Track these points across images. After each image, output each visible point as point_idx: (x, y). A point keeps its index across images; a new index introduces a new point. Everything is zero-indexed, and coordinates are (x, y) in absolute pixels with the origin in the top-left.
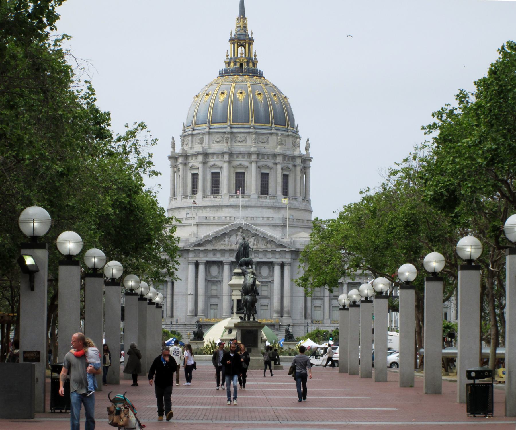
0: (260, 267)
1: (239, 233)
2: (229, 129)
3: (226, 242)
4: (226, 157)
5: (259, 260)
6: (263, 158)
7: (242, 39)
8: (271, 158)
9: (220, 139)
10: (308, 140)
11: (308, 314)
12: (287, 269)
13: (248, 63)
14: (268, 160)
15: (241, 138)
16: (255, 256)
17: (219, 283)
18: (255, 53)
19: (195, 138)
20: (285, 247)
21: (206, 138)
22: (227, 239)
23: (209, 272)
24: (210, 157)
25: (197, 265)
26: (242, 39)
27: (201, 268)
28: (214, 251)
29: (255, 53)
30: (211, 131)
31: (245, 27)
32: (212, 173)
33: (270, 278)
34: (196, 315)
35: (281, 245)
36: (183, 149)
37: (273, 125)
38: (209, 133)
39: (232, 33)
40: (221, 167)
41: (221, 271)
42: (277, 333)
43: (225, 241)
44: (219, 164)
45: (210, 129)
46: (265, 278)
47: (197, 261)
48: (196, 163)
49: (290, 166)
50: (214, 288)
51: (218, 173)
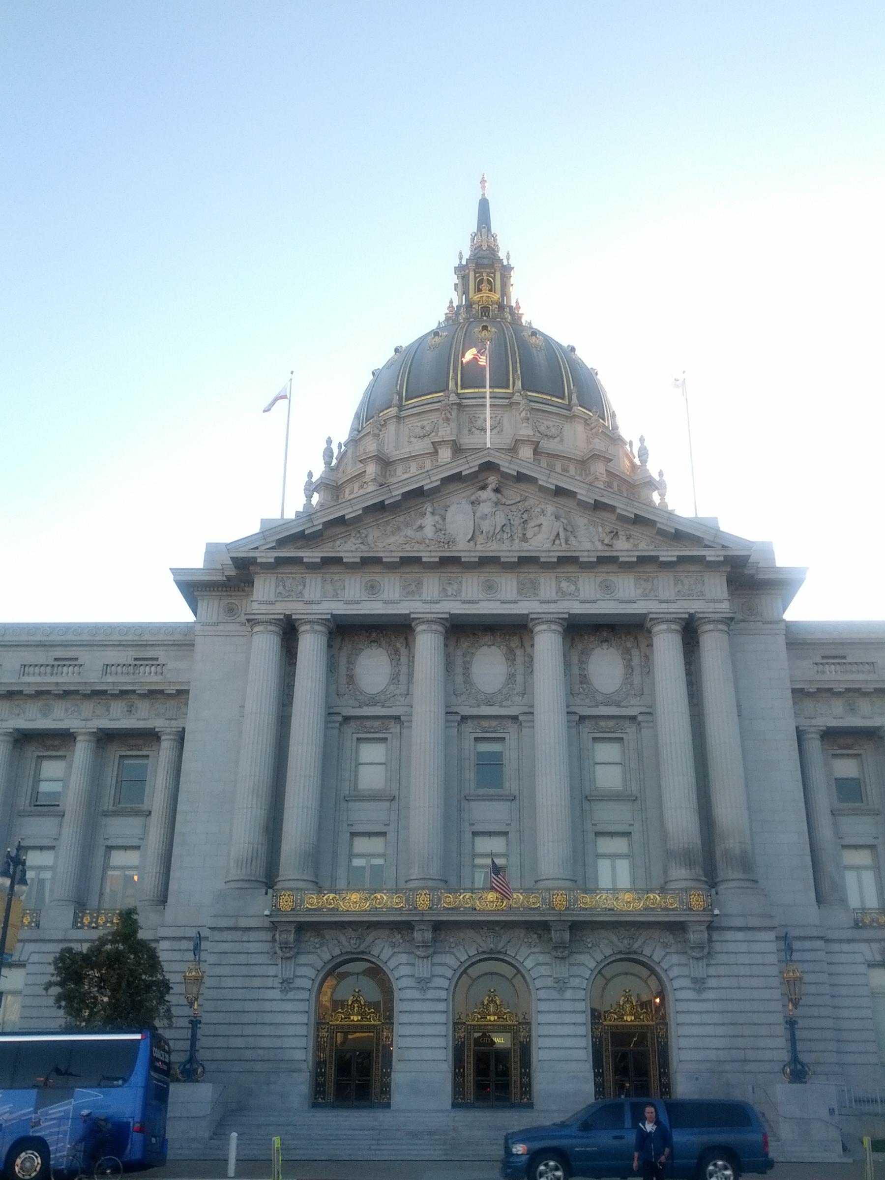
0: (585, 654)
1: (484, 495)
2: (453, 398)
5: (577, 608)
7: (484, 270)
8: (572, 470)
16: (559, 590)
17: (394, 728)
21: (392, 427)
22: (429, 522)
24: (400, 469)
25: (289, 631)
26: (484, 270)
30: (404, 414)
31: (492, 251)
33: (634, 701)
34: (269, 879)
38: (398, 418)
39: (461, 259)
41: (404, 669)
42: (699, 970)
43: (421, 528)
47: (288, 617)
50: (371, 753)
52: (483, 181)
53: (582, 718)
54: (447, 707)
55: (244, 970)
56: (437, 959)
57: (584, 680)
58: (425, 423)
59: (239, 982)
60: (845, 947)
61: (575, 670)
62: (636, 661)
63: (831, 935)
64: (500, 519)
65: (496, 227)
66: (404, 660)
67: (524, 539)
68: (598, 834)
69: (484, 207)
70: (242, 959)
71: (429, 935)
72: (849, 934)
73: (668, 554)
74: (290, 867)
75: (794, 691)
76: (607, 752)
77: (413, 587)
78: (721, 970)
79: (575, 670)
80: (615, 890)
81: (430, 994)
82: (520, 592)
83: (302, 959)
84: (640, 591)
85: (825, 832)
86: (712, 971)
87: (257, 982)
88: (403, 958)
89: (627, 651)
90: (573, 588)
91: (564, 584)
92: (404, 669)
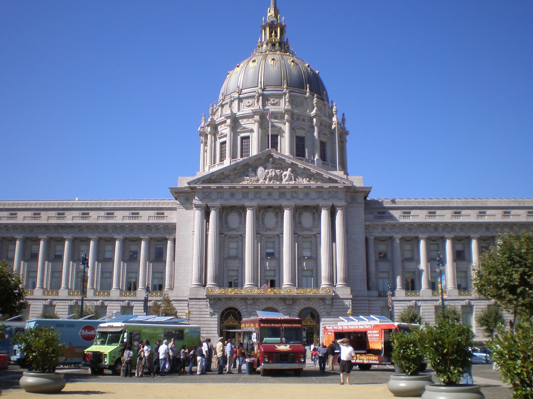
0: (300, 215)
1: (269, 165)
2: (260, 91)
4: (257, 117)
6: (298, 119)
9: (251, 103)
10: (343, 115)
11: (371, 285)
13: (280, 44)
14: (303, 122)
15: (274, 101)
16: (292, 196)
18: (287, 39)
19: (225, 108)
20: (336, 181)
23: (226, 223)
28: (233, 192)
29: (287, 39)
32: (243, 138)
35: (330, 179)
36: (212, 119)
37: (308, 90)
40: (252, 131)
44: (250, 126)
45: (240, 94)
46: (307, 229)
48: (225, 130)
49: (327, 133)
50: (233, 245)
51: (248, 138)
53: (299, 235)
54: (257, 231)
55: (199, 310)
57: (300, 223)
58: (249, 100)
59: (197, 313)
60: (375, 302)
61: (297, 220)
64: (274, 174)
66: (243, 217)
67: (282, 180)
70: (198, 306)
73: (327, 185)
74: (210, 282)
75: (366, 225)
76: (307, 245)
77: (246, 195)
78: (335, 310)
79: (297, 220)
82: (280, 197)
84: (317, 196)
85: (373, 269)
86: (333, 310)
87: (203, 313)
88: (244, 307)
89: (314, 213)
90: (296, 195)
91: (294, 194)
92: (243, 220)
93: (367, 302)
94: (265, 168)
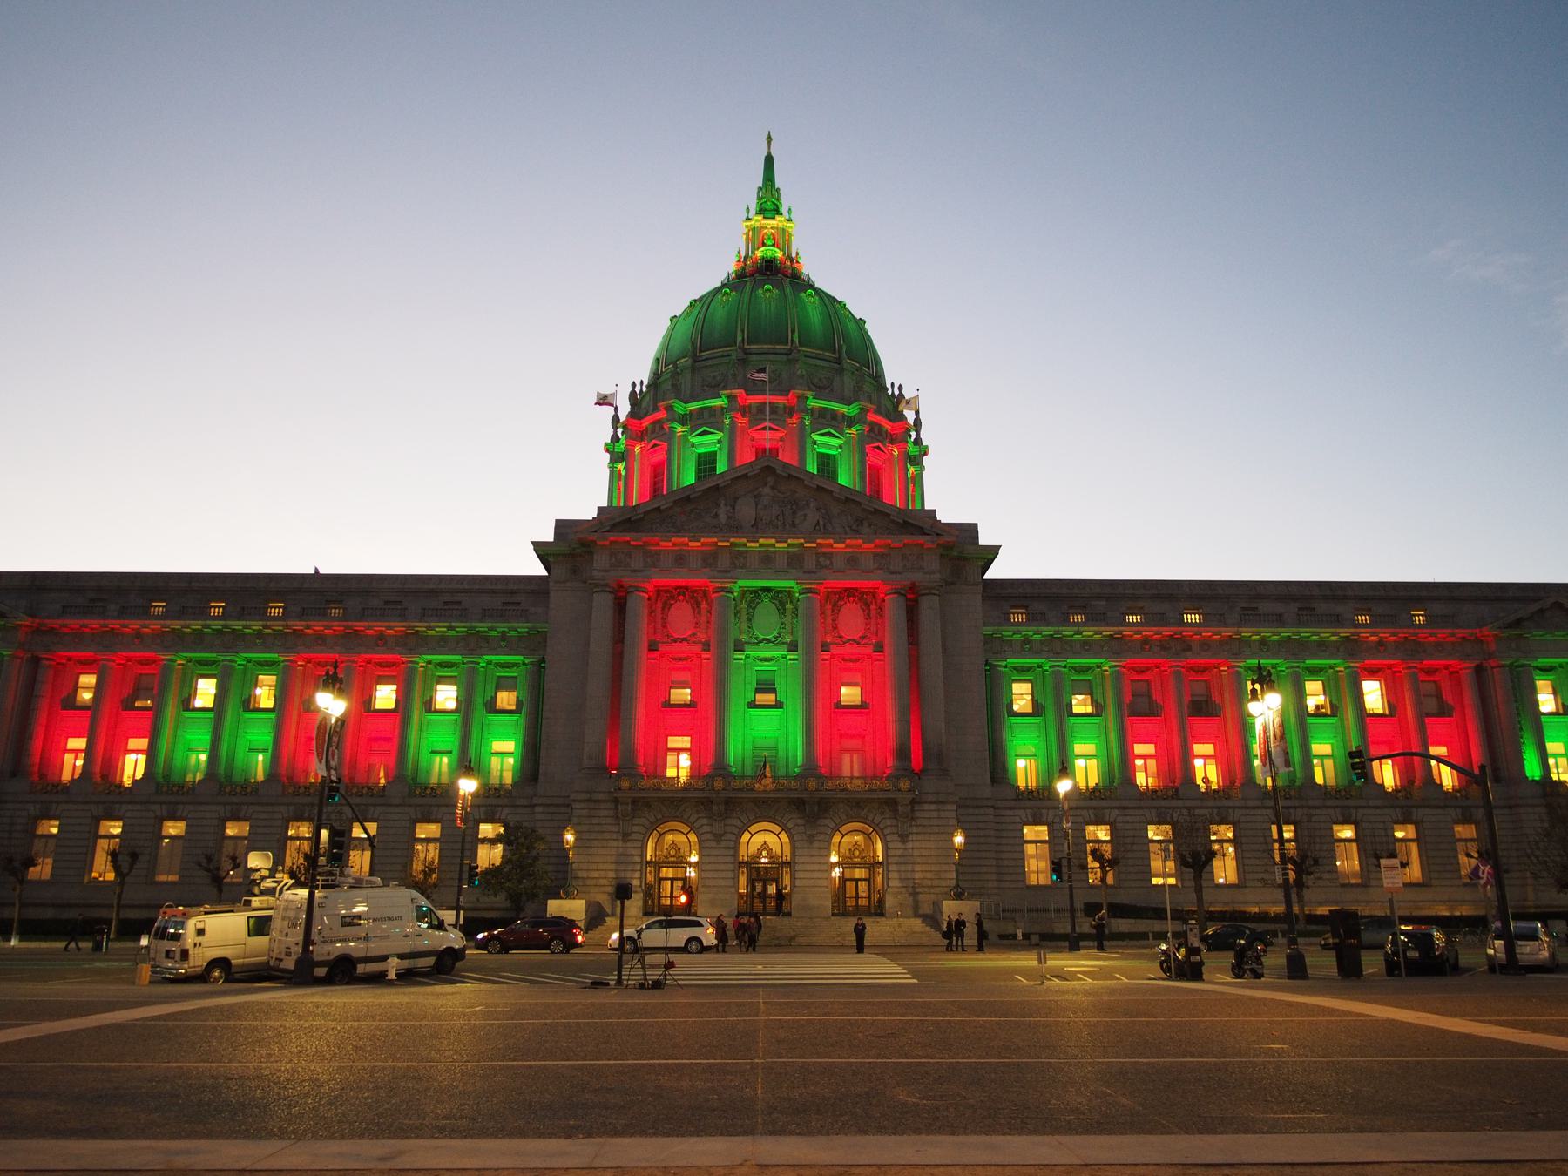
1: (767, 490)
3: (723, 518)
12: (928, 610)
16: (818, 564)
27: (638, 606)
41: (703, 619)
43: (716, 515)
52: (769, 139)
56: (729, 821)
60: (1009, 812)
61: (829, 620)
62: (873, 613)
63: (1000, 804)
65: (779, 182)
66: (704, 612)
68: (841, 736)
69: (769, 161)
71: (722, 808)
72: (1013, 803)
80: (852, 778)
81: (723, 844)
83: (636, 821)
88: (705, 821)
93: (991, 811)
94: (758, 497)
